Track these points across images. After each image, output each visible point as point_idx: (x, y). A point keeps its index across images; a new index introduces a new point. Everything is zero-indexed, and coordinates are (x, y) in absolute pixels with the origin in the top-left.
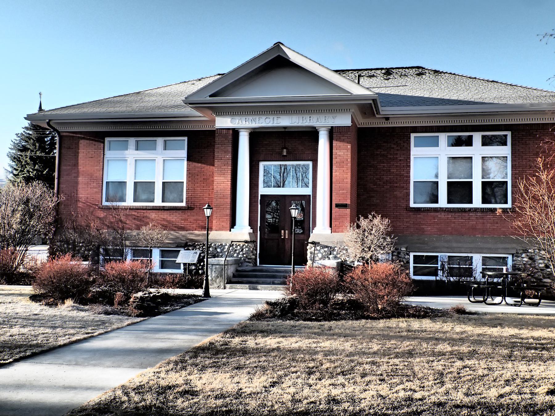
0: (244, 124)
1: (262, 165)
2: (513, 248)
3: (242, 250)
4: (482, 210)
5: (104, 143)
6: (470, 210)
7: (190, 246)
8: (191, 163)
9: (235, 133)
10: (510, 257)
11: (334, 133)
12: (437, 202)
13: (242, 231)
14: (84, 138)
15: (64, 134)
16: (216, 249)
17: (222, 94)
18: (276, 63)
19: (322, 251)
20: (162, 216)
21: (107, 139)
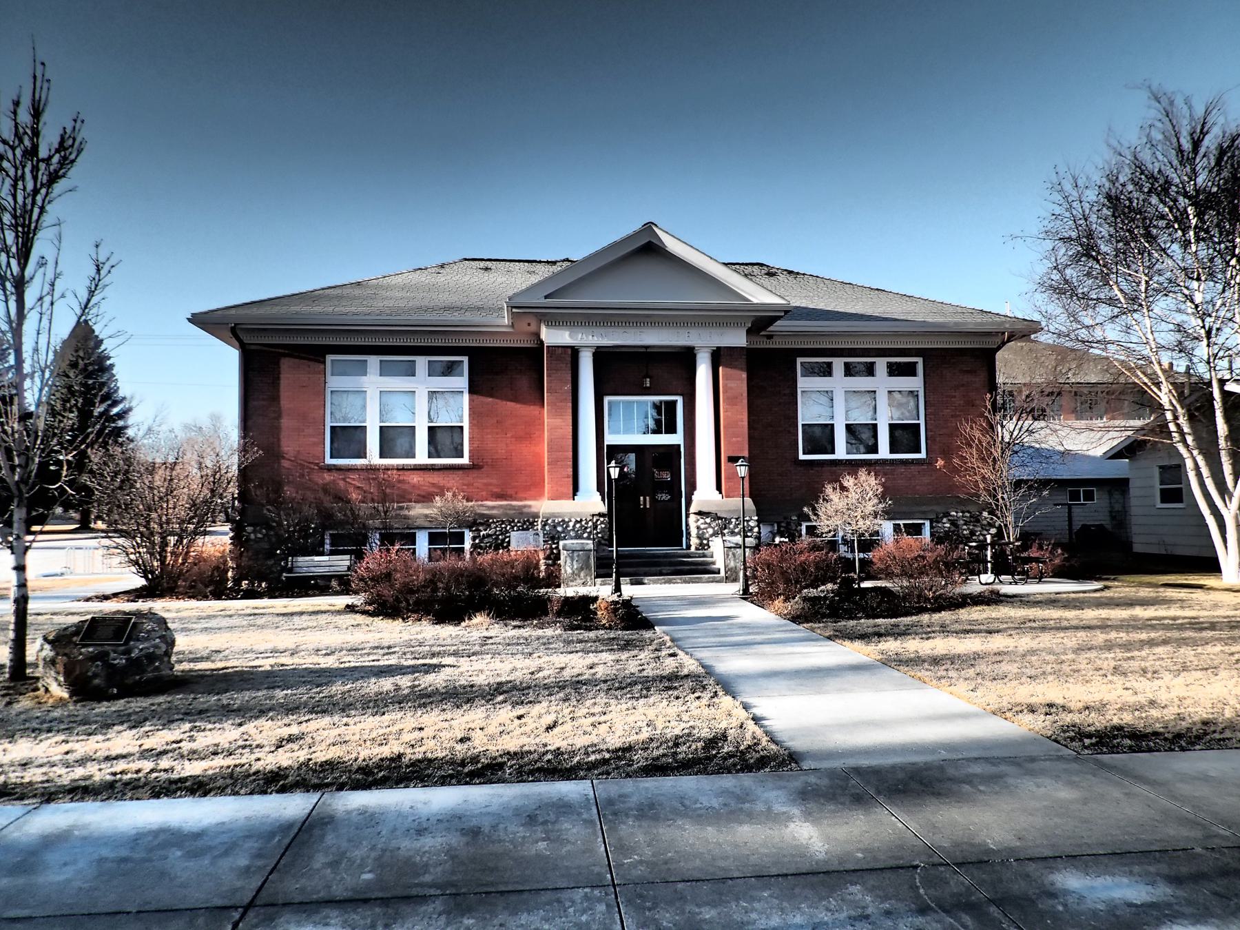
0: (587, 339)
1: (607, 399)
2: (932, 511)
3: (595, 528)
4: (892, 462)
5: (324, 363)
6: (877, 462)
7: (481, 524)
8: (475, 396)
9: (573, 353)
10: (927, 523)
11: (719, 357)
12: (876, 452)
13: (590, 502)
14: (285, 355)
15: (253, 347)
16: (555, 527)
17: (568, 290)
18: (646, 249)
19: (713, 524)
20: (431, 480)
21: (330, 358)
